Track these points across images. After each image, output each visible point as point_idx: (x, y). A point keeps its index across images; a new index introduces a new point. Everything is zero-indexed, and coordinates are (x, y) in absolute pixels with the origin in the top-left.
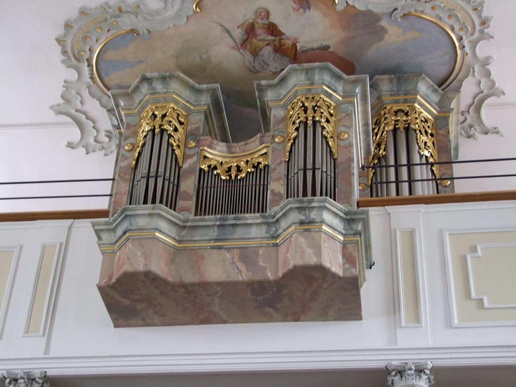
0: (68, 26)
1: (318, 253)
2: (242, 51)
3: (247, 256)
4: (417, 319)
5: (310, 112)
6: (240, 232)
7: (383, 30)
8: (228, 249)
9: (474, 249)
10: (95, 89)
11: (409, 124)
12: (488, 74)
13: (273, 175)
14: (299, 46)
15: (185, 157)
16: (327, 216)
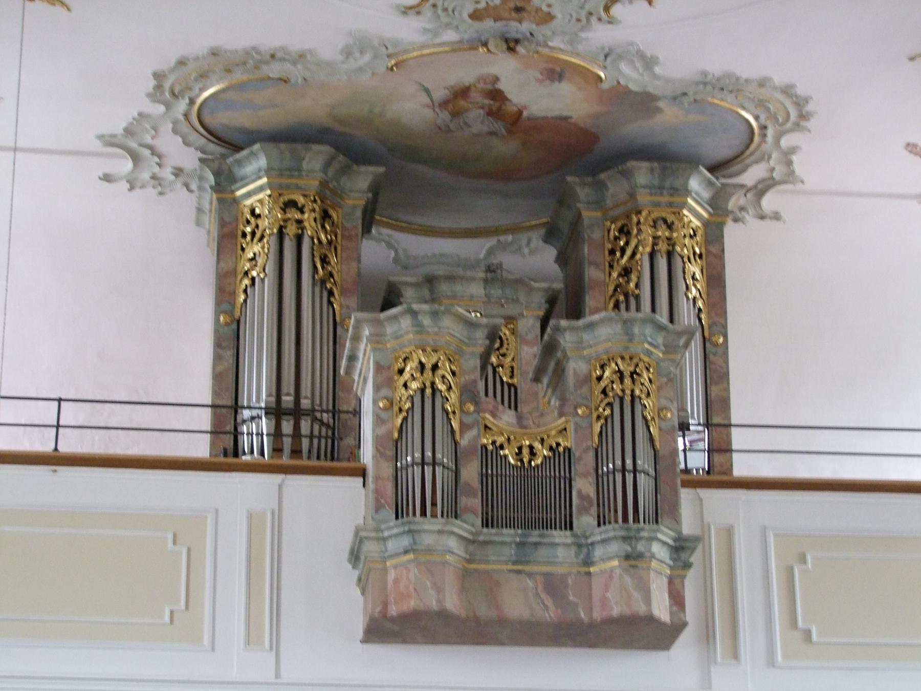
0: (181, 63)
1: (648, 600)
2: (438, 110)
3: (554, 586)
4: (735, 654)
5: (628, 381)
6: (542, 552)
7: (659, 110)
8: (530, 575)
9: (803, 559)
10: (184, 127)
11: (674, 245)
12: (789, 163)
13: (578, 468)
14: (525, 114)
15: (464, 427)
16: (656, 548)
